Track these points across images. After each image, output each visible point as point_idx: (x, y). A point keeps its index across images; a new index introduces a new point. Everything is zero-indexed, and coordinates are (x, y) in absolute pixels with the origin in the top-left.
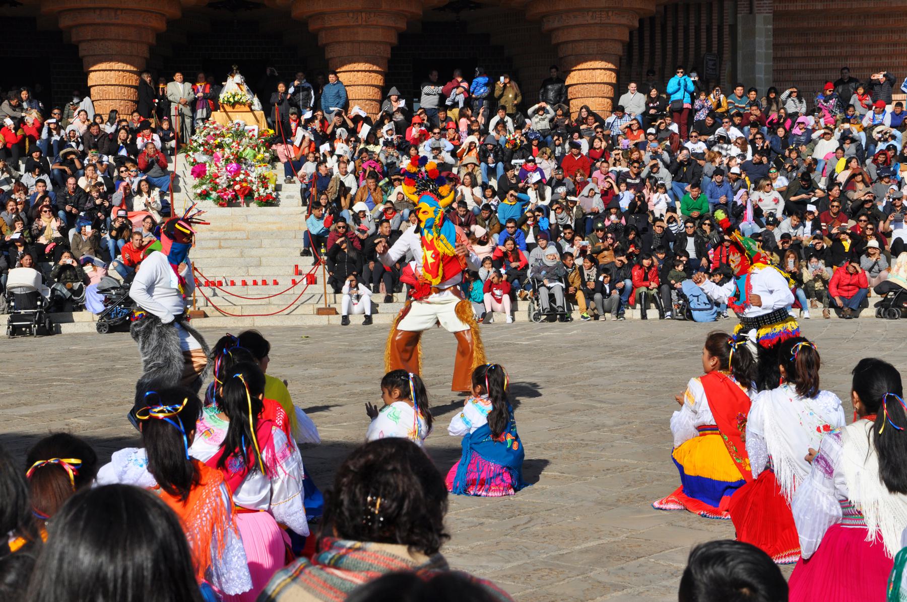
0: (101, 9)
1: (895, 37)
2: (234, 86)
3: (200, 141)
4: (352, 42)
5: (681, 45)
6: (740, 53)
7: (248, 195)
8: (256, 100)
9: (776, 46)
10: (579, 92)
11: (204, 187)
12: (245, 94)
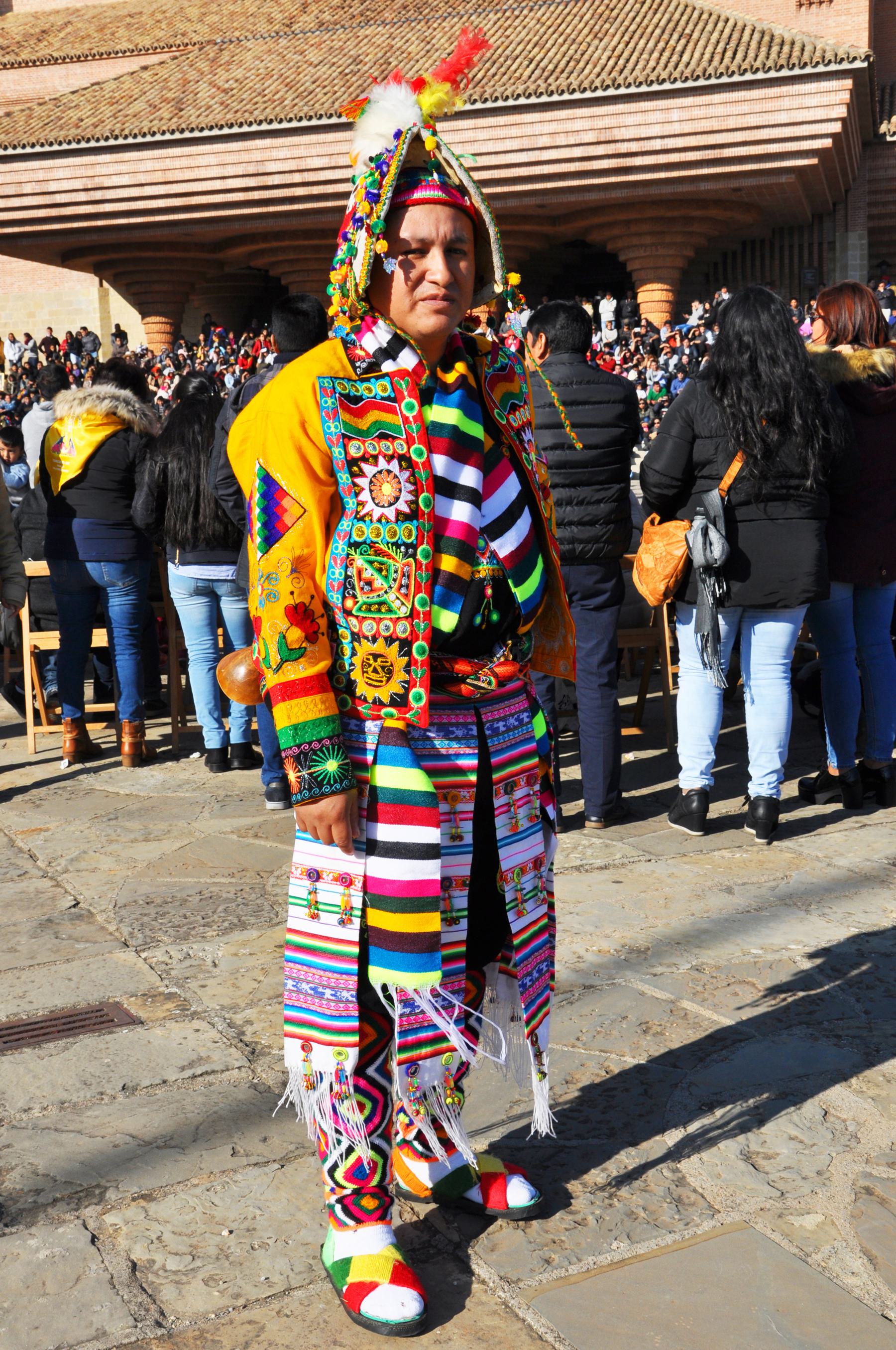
0: (299, 271)
5: (787, 261)
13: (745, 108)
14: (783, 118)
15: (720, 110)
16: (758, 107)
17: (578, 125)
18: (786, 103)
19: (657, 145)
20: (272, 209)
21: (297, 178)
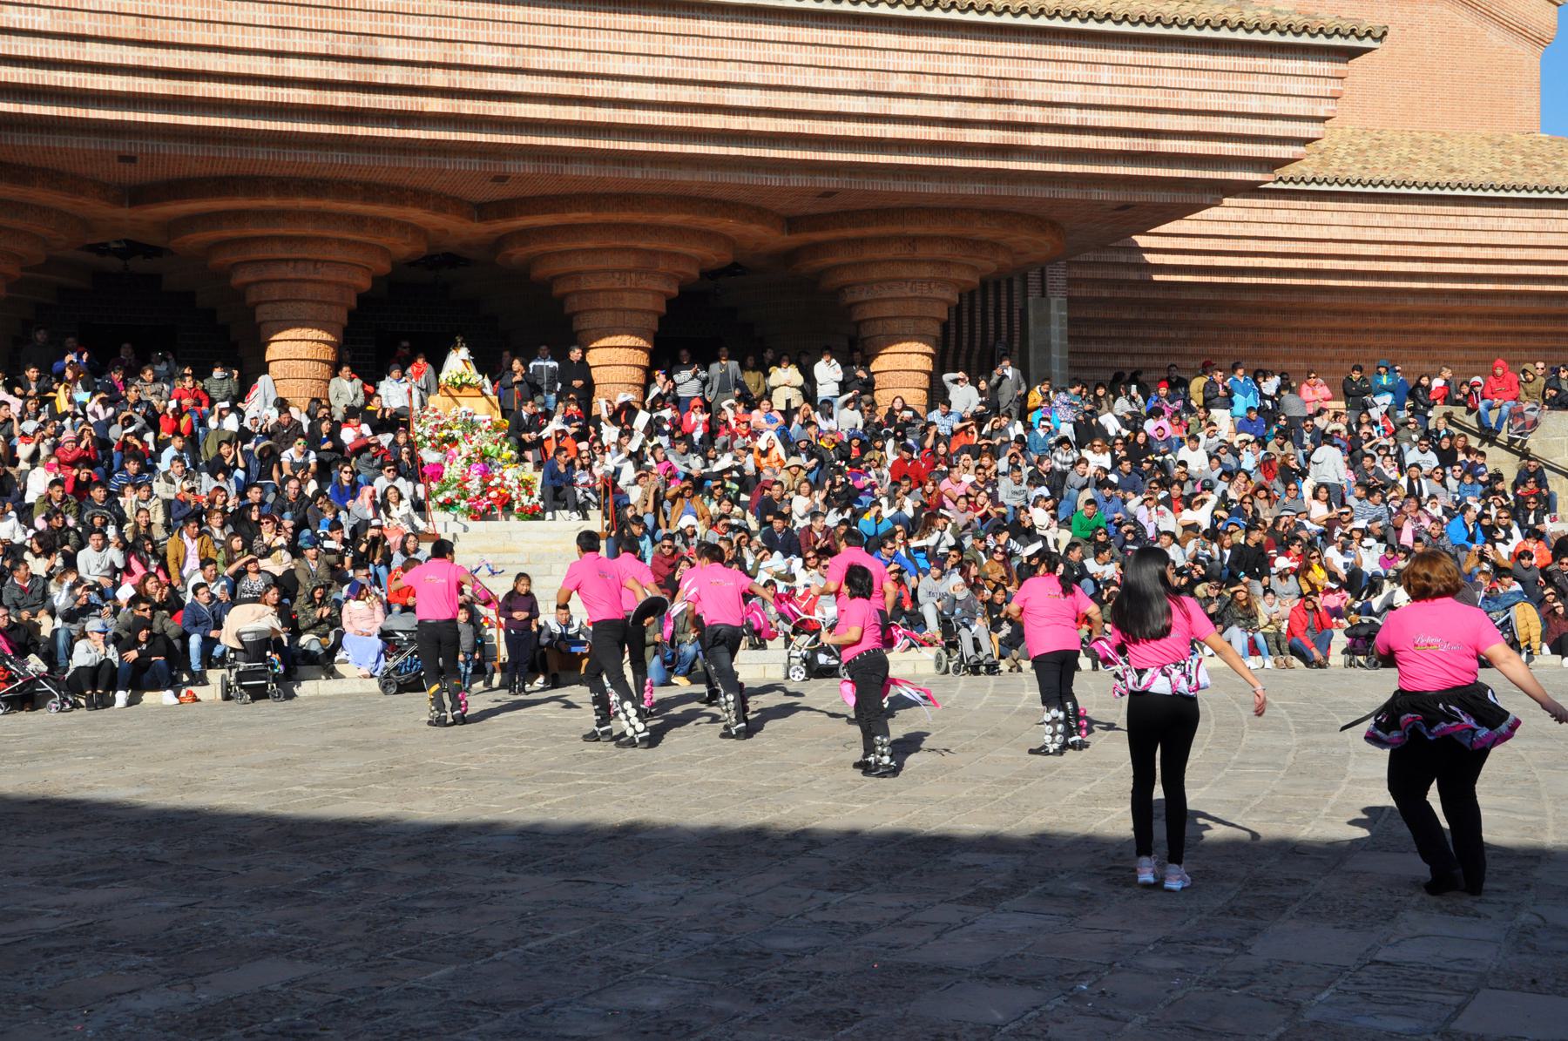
0: (296, 260)
1: (1172, 335)
2: (458, 362)
3: (427, 434)
4: (615, 310)
6: (1032, 343)
7: (507, 505)
8: (487, 381)
9: (1070, 338)
11: (448, 494)
12: (474, 376)
13: (1204, 81)
14: (1254, 105)
15: (1170, 78)
16: (1222, 82)
17: (958, 65)
18: (1261, 83)
19: (1072, 117)
20: (361, 131)
21: (438, 78)
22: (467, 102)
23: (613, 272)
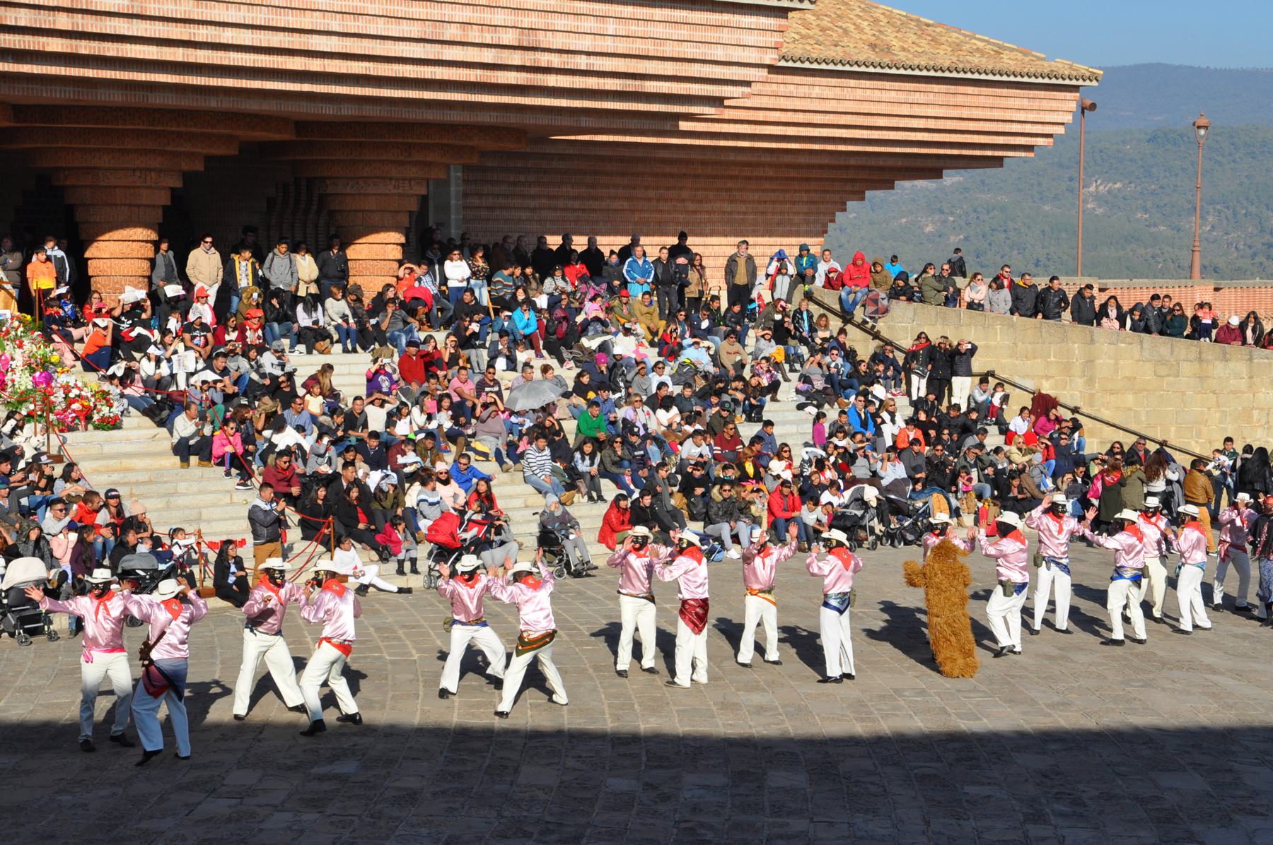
1: (522, 178)
4: (131, 205)
10: (366, 269)
13: (683, 33)
14: (719, 53)
15: (659, 31)
16: (698, 34)
18: (725, 35)
19: (582, 62)
22: (84, 43)
23: (134, 170)
